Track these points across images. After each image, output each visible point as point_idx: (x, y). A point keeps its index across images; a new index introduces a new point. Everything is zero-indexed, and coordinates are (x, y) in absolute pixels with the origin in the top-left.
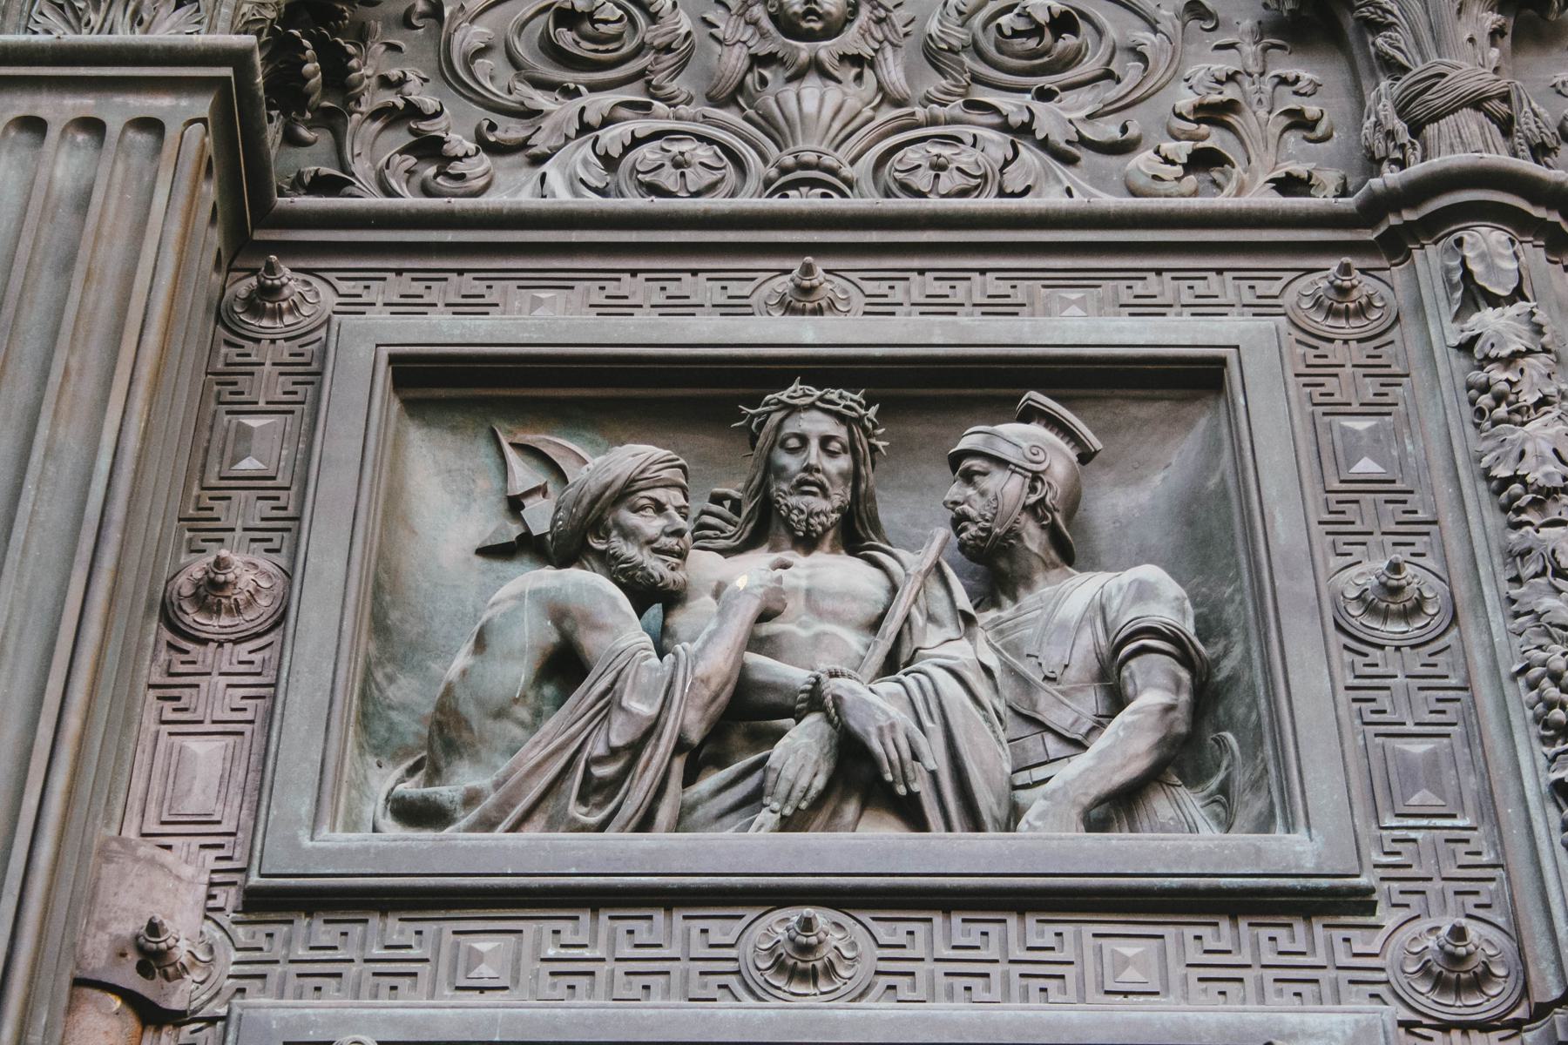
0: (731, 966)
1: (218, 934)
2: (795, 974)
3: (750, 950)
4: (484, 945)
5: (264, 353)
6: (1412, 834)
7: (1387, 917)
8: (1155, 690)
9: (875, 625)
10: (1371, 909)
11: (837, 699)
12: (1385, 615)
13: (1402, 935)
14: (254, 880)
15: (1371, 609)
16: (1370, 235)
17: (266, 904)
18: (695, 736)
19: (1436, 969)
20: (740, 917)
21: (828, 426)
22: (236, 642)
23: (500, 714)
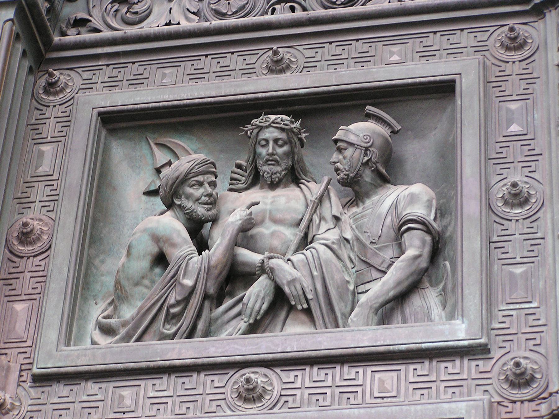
0: (222, 396)
1: (24, 393)
2: (246, 400)
3: (230, 388)
4: (126, 392)
5: (48, 112)
6: (511, 313)
7: (496, 353)
8: (416, 245)
9: (298, 224)
10: (489, 351)
11: (272, 270)
12: (513, 206)
13: (499, 364)
14: (35, 370)
15: (506, 203)
16: (527, 7)
17: (43, 380)
18: (212, 290)
19: (511, 378)
20: (228, 373)
21: (276, 134)
22: (35, 256)
23: (137, 284)
